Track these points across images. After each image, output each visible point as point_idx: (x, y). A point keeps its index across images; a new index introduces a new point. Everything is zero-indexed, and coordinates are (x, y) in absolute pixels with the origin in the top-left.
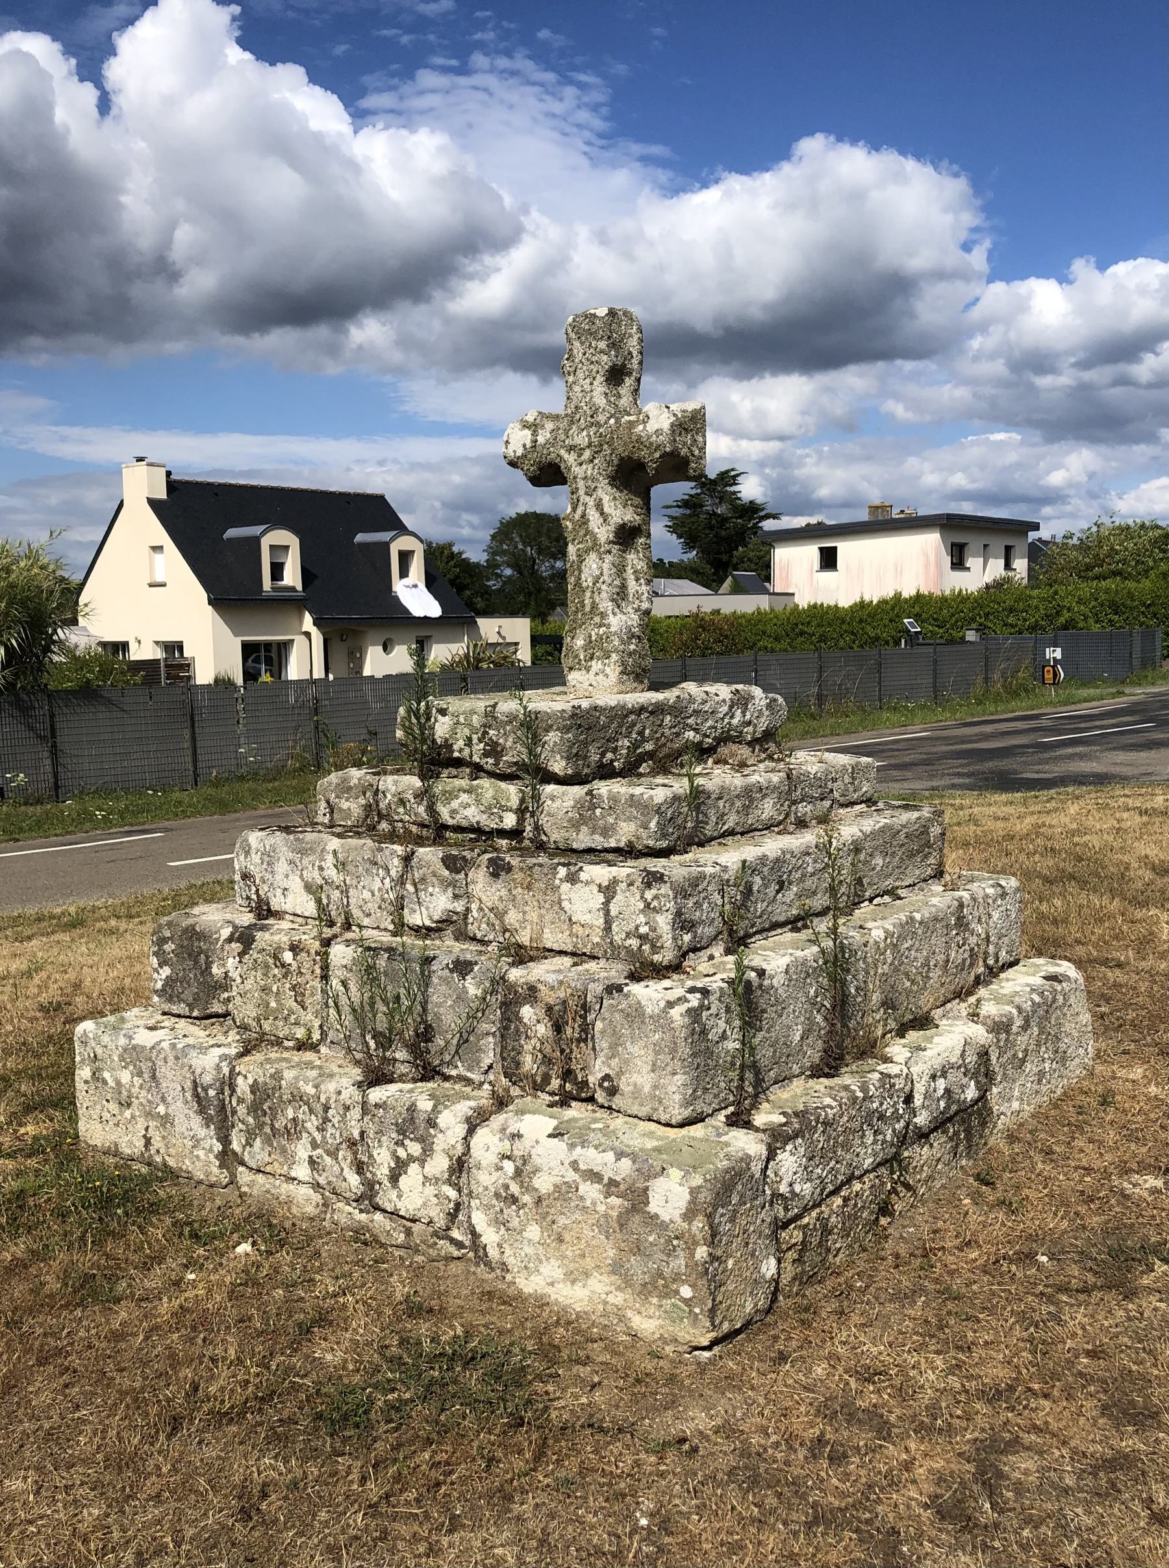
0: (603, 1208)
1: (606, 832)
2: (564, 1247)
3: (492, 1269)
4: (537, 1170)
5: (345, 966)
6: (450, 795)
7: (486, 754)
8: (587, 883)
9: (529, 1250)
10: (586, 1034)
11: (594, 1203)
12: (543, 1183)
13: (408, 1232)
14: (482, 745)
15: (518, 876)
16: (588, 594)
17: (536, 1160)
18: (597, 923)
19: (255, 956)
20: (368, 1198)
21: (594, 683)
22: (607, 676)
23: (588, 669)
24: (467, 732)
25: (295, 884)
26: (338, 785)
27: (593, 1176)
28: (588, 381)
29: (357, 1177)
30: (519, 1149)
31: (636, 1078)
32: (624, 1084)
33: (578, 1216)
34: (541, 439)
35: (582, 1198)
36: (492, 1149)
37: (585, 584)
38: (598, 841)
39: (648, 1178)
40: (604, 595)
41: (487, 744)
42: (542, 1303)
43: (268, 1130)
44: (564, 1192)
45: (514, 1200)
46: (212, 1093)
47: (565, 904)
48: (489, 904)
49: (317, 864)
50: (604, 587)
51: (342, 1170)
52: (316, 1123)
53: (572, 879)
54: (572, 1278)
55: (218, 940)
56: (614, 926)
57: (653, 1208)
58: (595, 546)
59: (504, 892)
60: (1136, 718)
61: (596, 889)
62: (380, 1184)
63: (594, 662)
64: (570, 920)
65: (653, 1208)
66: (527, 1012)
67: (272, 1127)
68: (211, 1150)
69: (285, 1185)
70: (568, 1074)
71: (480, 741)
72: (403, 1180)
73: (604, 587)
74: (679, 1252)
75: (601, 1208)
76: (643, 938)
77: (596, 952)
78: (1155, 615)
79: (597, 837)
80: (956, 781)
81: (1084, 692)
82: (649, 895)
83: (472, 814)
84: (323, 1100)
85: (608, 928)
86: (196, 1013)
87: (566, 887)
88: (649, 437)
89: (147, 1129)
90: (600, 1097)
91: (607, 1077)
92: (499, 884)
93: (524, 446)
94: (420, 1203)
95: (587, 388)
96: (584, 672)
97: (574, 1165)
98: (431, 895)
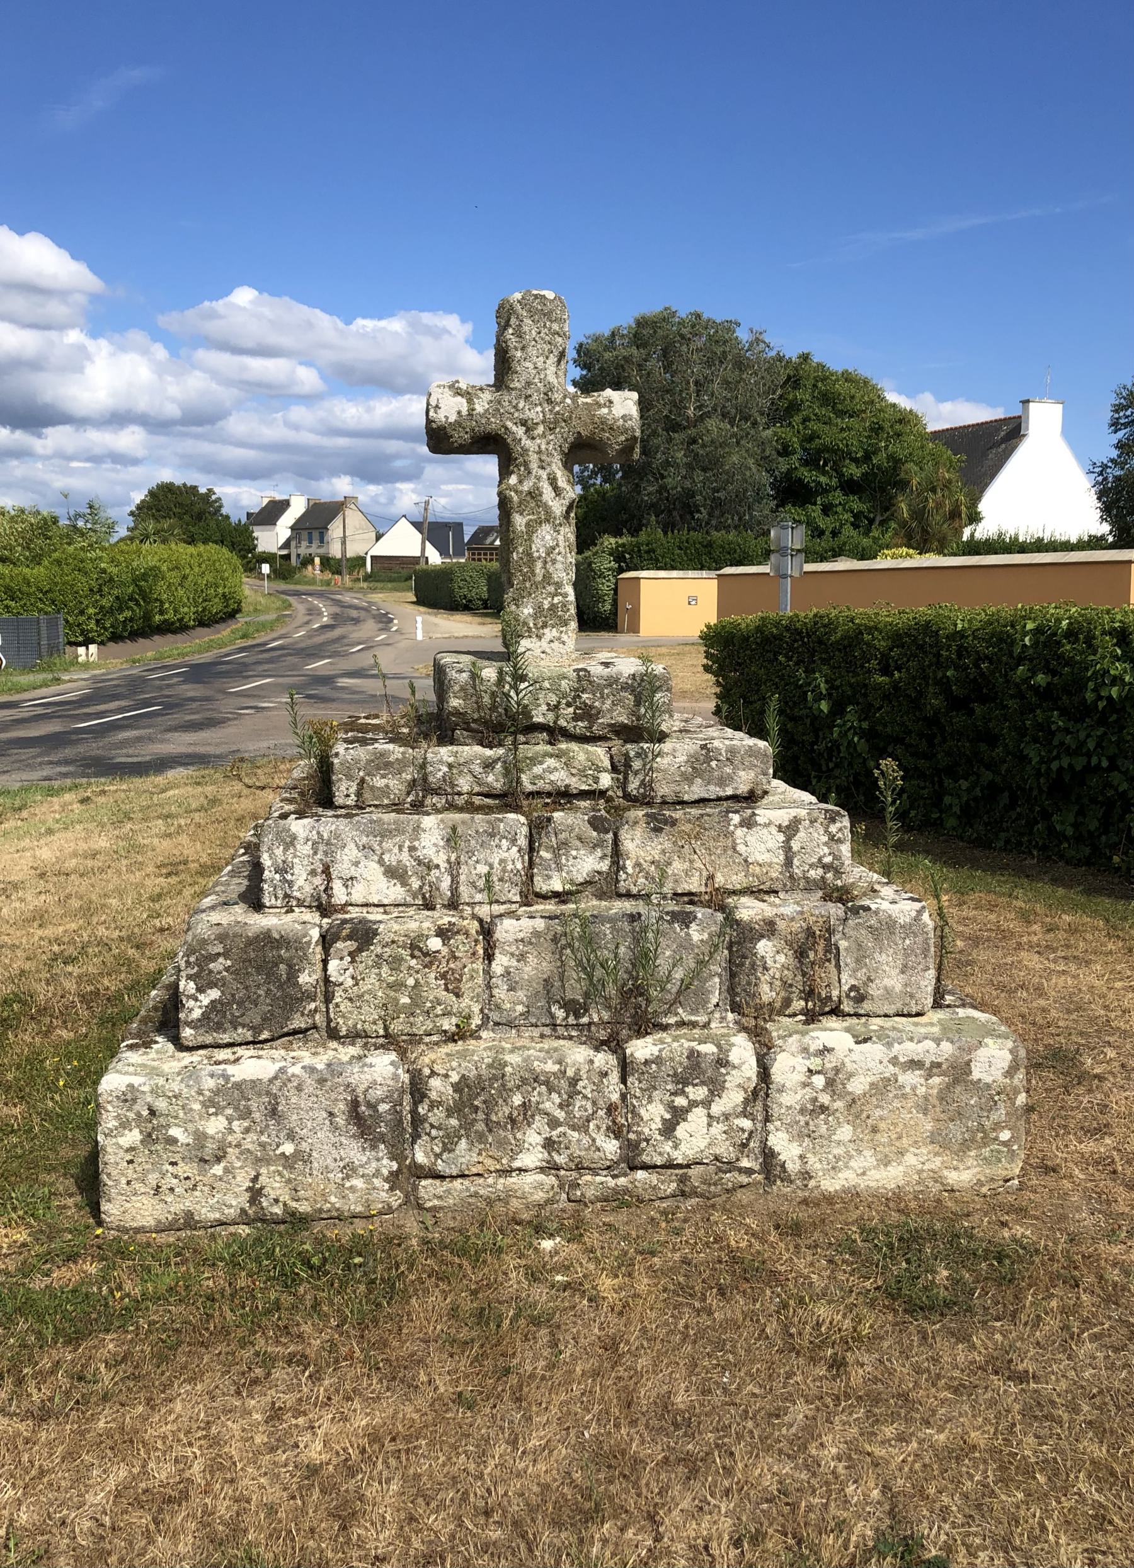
0: (924, 1089)
1: (722, 782)
2: (878, 1136)
3: (791, 1182)
4: (851, 1075)
5: (522, 940)
6: (534, 761)
7: (576, 718)
8: (767, 825)
9: (838, 1151)
10: (832, 952)
11: (914, 1088)
12: (857, 1086)
13: (683, 1179)
14: (571, 710)
15: (687, 827)
16: (539, 564)
17: (850, 1067)
18: (776, 860)
19: (379, 950)
20: (631, 1160)
21: (548, 650)
22: (564, 643)
23: (539, 637)
24: (553, 699)
25: (372, 870)
26: (369, 762)
27: (914, 1064)
28: (541, 359)
29: (614, 1142)
30: (830, 1062)
31: (888, 982)
32: (873, 990)
33: (896, 1104)
34: (479, 408)
35: (902, 1087)
36: (798, 1068)
37: (536, 555)
38: (714, 791)
39: (970, 1052)
40: (559, 566)
41: (577, 708)
42: (852, 1196)
43: (480, 1126)
44: (882, 1087)
45: (824, 1109)
46: (383, 1107)
47: (741, 848)
48: (649, 858)
49: (407, 843)
50: (559, 558)
51: (594, 1140)
52: (558, 1101)
53: (748, 823)
54: (886, 1162)
55: (309, 943)
56: (796, 862)
57: (976, 1075)
58: (549, 518)
59: (668, 845)
60: (123, 703)
61: (774, 830)
62: (647, 1141)
63: (546, 631)
64: (746, 861)
65: (976, 1075)
66: (764, 947)
67: (487, 1121)
68: (377, 1173)
69: (502, 1180)
70: (809, 994)
71: (569, 705)
72: (681, 1131)
73: (559, 558)
74: (1001, 1105)
75: (921, 1091)
76: (826, 867)
77: (778, 886)
78: (53, 602)
79: (712, 788)
80: (64, 769)
81: (25, 679)
82: (833, 829)
83: (561, 777)
84: (570, 1073)
85: (788, 862)
86: (265, 1035)
87: (740, 833)
88: (615, 420)
89: (255, 1179)
90: (847, 1007)
91: (853, 988)
92: (663, 838)
93: (459, 413)
94: (705, 1143)
95: (540, 365)
96: (534, 639)
97: (894, 1061)
98: (575, 858)
